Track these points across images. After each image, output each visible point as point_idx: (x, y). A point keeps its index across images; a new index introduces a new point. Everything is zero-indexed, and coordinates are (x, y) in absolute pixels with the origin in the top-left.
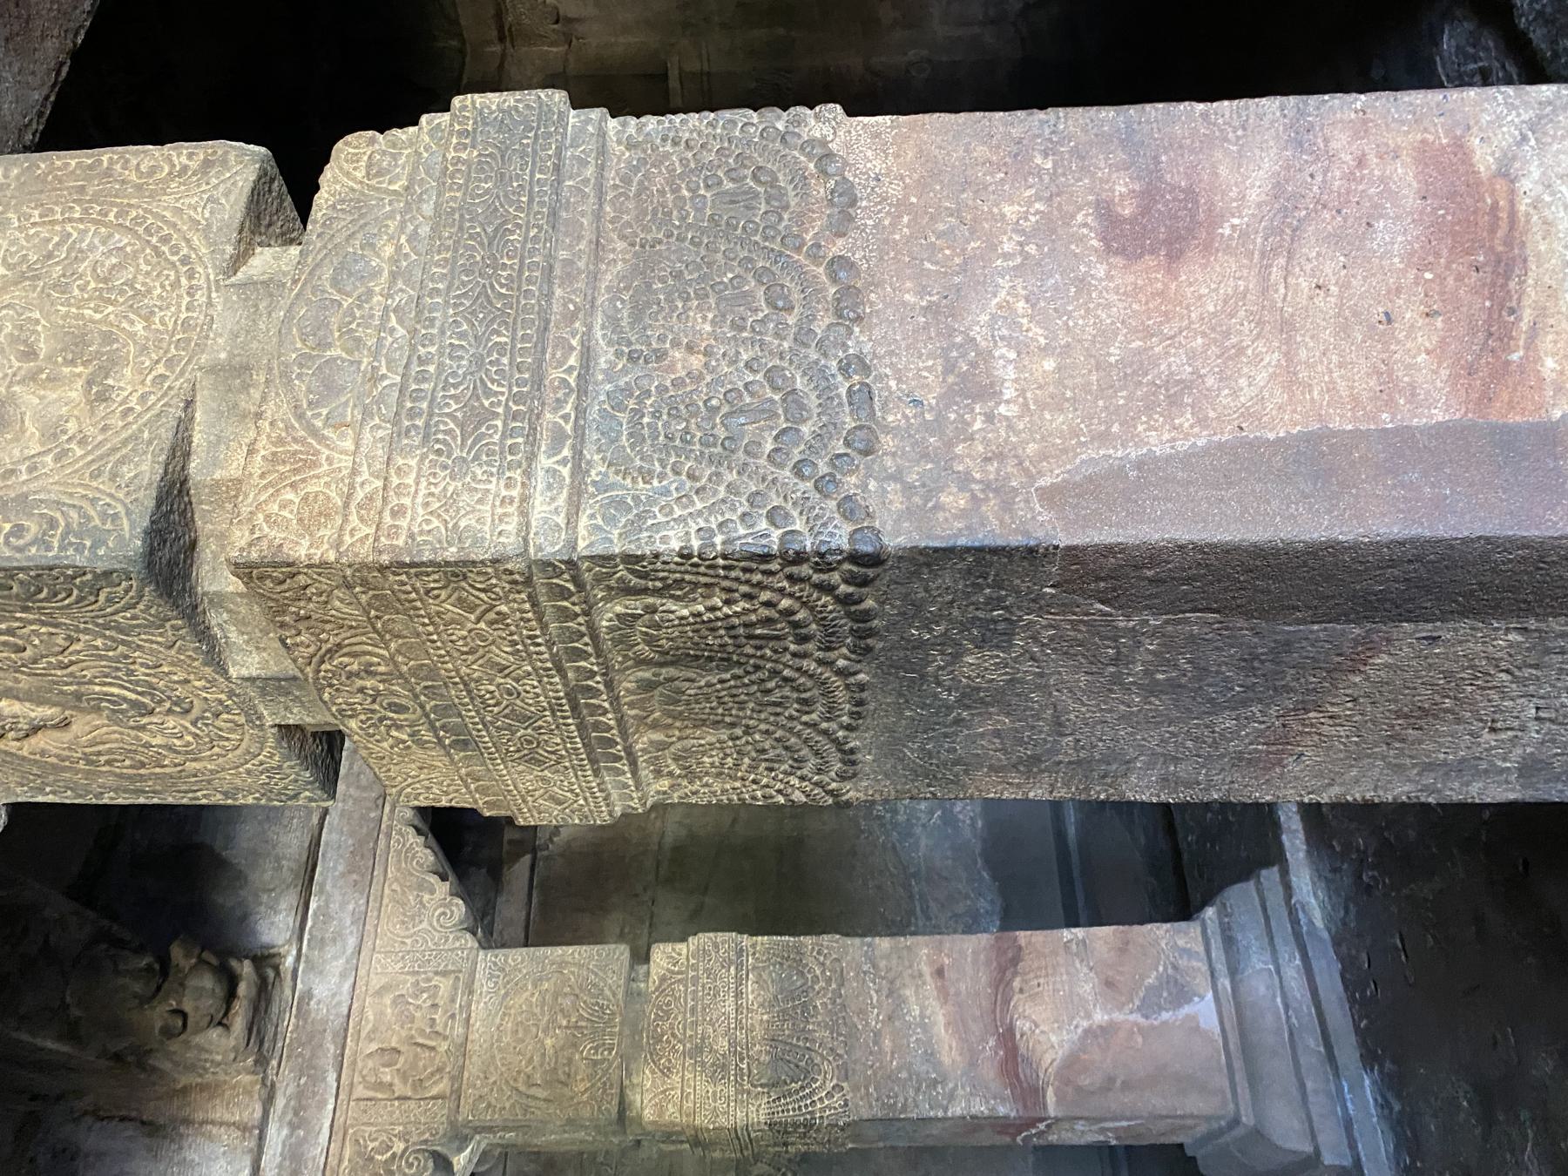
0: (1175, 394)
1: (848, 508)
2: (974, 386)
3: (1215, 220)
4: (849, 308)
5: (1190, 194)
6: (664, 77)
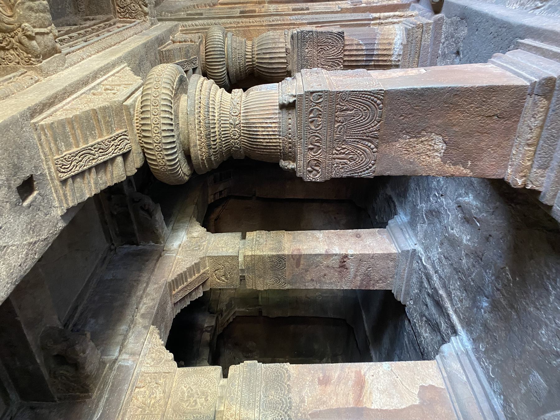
0: (324, 403)
1: (288, 416)
2: (303, 401)
3: (331, 380)
4: (289, 392)
5: (329, 377)
6: (258, 298)
